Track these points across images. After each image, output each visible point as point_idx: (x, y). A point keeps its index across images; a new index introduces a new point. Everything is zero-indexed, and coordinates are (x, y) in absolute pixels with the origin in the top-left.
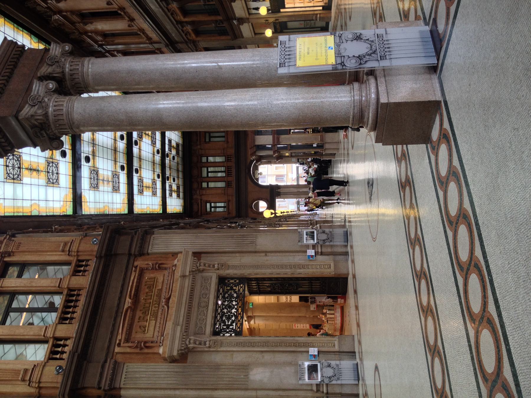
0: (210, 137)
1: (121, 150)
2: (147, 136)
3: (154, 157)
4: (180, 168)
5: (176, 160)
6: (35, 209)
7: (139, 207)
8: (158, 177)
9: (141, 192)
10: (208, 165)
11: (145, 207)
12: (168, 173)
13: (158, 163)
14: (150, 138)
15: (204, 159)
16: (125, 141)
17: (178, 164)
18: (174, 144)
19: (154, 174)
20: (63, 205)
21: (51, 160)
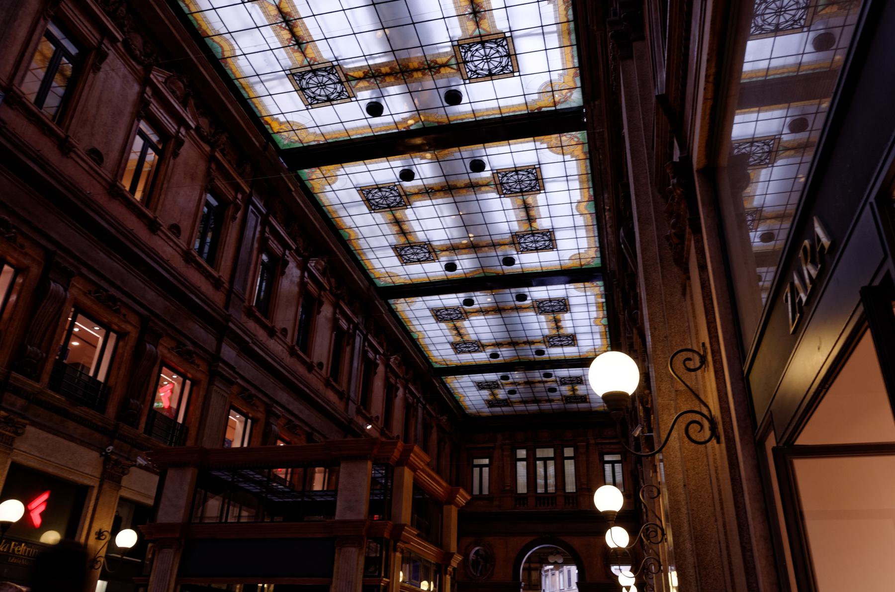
0: (613, 463)
1: (486, 262)
2: (553, 325)
3: (525, 343)
4: (546, 406)
5: (552, 395)
6: (221, 47)
7: (410, 315)
8: (494, 356)
9: (439, 315)
10: (559, 460)
11: (419, 328)
12: (517, 376)
13: (521, 353)
14: (554, 332)
15: (569, 452)
16: (508, 269)
17: (550, 401)
18: (581, 390)
19: (493, 345)
20: (281, 123)
21: (343, 79)
